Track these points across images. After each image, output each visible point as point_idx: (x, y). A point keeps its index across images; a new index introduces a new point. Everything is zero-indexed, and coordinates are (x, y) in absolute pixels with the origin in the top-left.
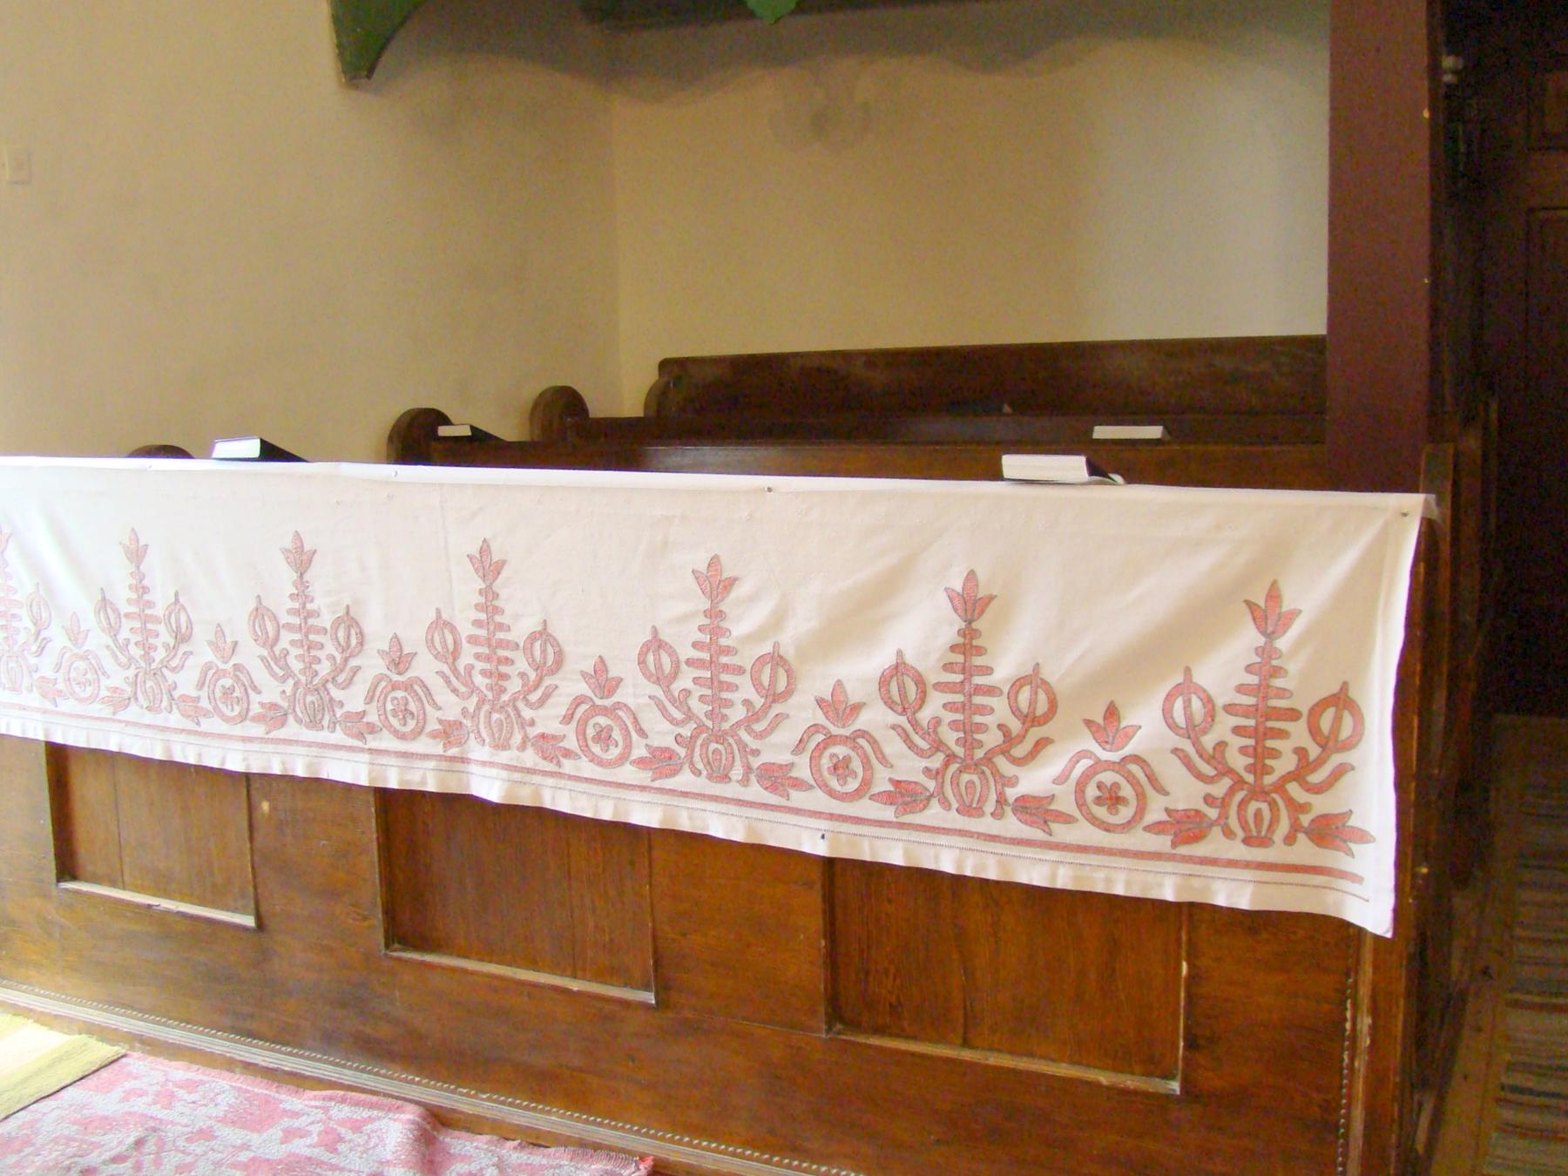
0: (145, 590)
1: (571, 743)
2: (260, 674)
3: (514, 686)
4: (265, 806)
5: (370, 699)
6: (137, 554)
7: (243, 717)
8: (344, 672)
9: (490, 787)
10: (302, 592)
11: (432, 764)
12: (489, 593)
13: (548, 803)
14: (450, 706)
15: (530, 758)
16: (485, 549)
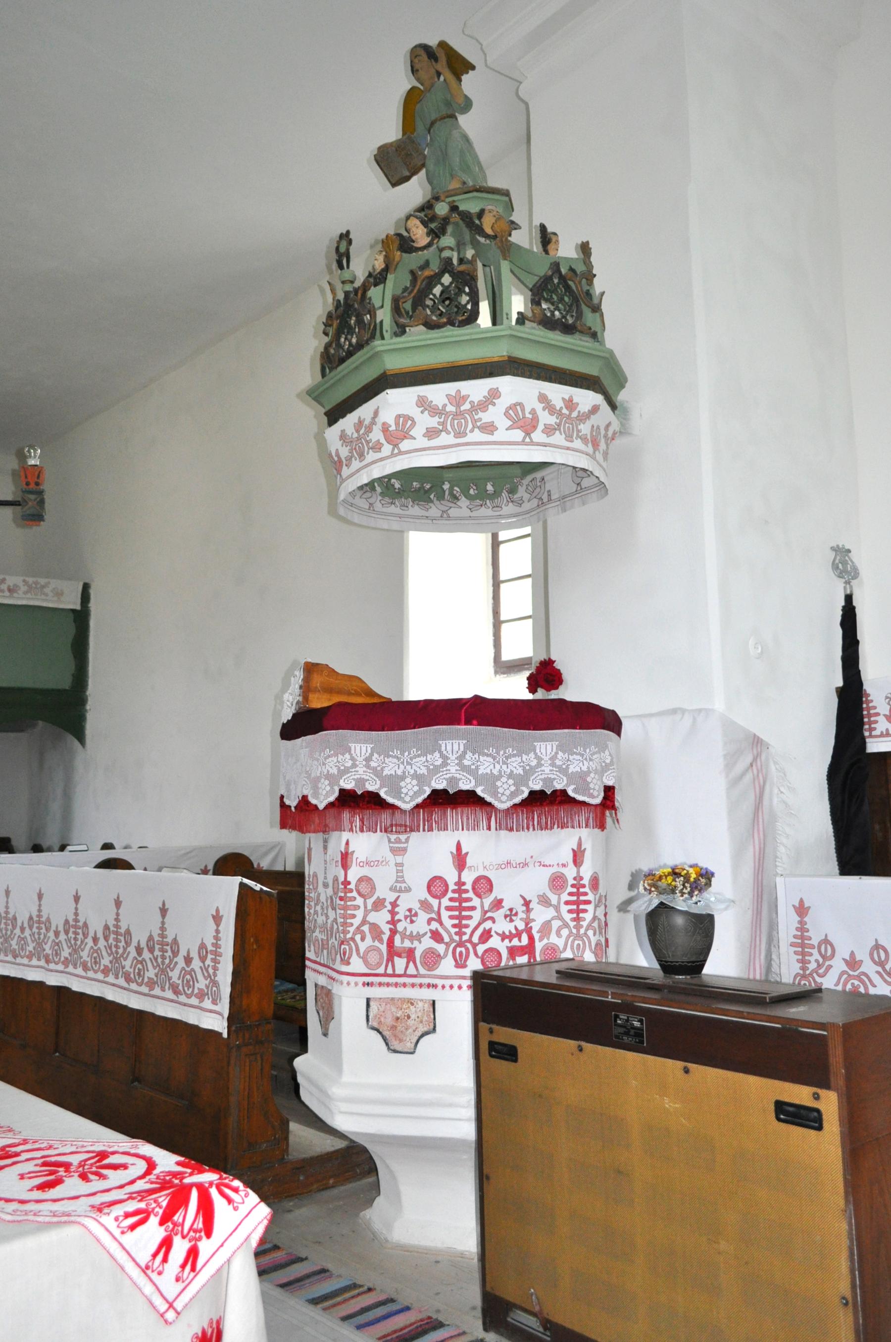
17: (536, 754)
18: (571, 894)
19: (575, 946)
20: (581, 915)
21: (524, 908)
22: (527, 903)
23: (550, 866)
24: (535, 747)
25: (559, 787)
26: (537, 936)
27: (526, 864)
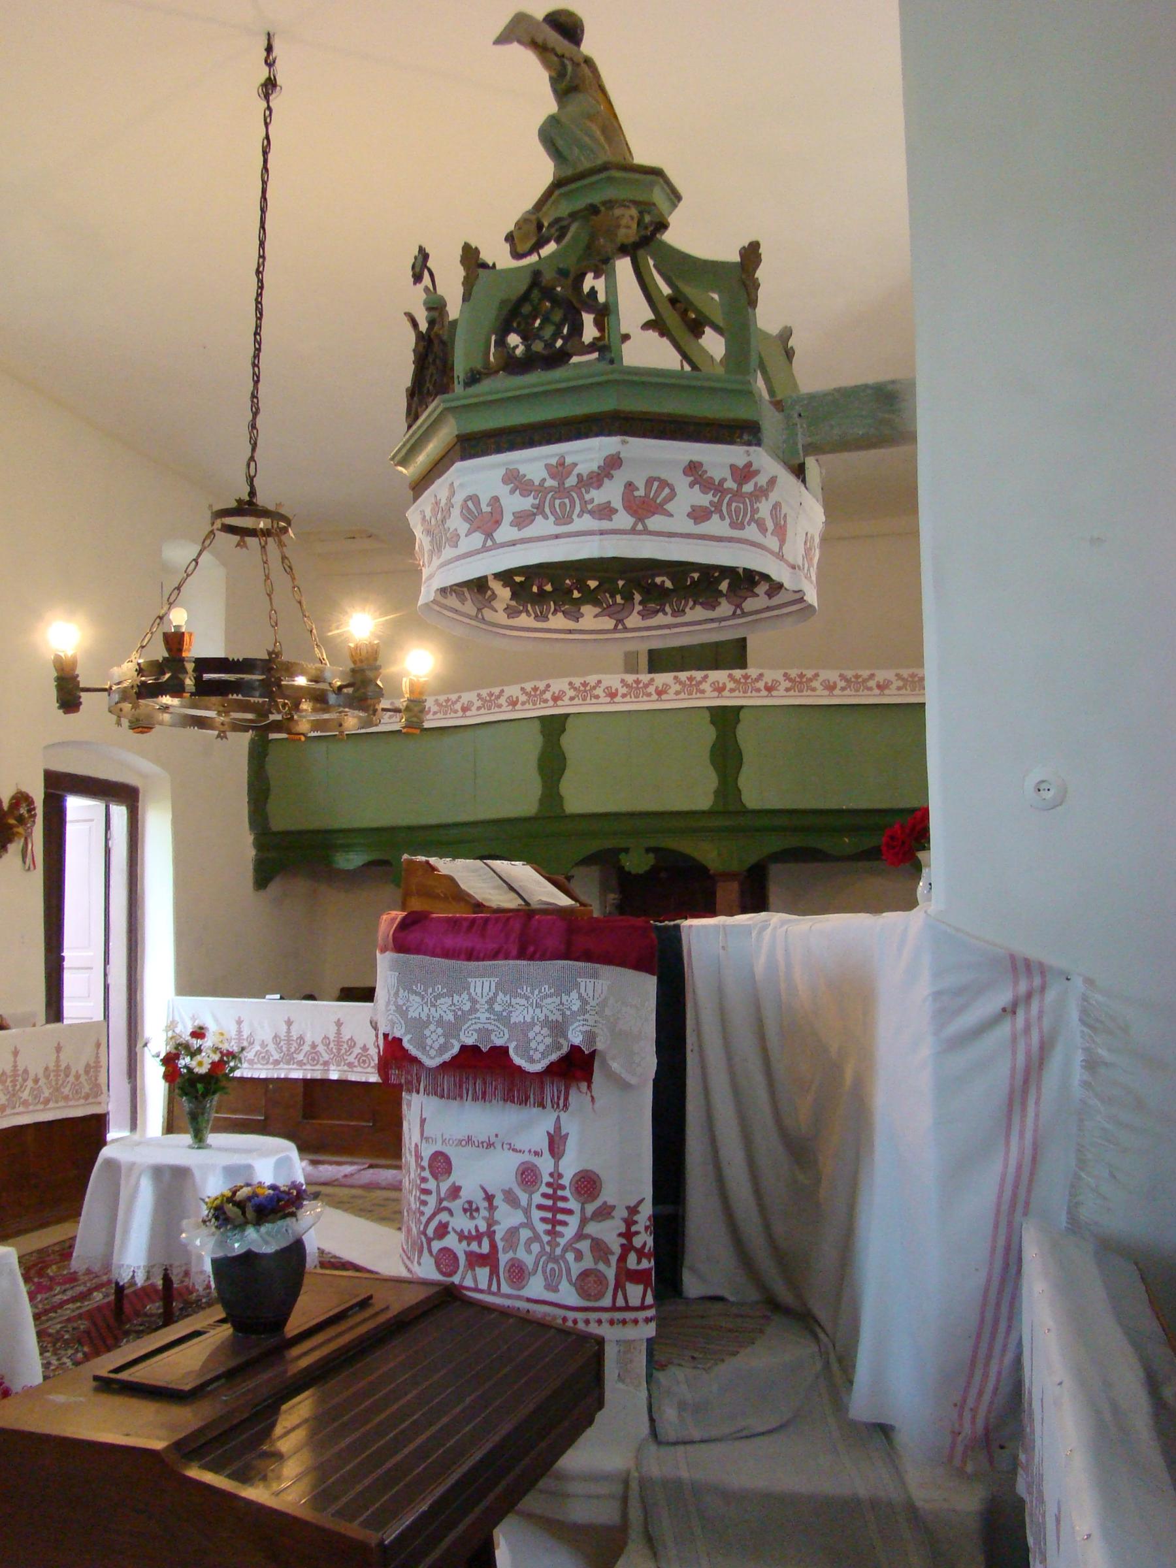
0: (242, 1032)
1: (356, 1064)
2: (274, 1052)
3: (343, 1051)
4: (271, 1086)
5: (304, 1056)
6: (239, 1022)
7: (267, 1063)
8: (298, 1051)
9: (334, 1076)
10: (289, 1031)
11: (320, 1072)
12: (339, 1030)
13: (349, 1079)
14: (326, 1057)
15: (346, 1068)
16: (339, 1020)
17: (469, 994)
18: (545, 1195)
19: (548, 1270)
20: (559, 1228)
21: (486, 1204)
22: (489, 1198)
23: (520, 1151)
24: (469, 984)
25: (499, 1042)
26: (500, 1245)
27: (490, 1145)
